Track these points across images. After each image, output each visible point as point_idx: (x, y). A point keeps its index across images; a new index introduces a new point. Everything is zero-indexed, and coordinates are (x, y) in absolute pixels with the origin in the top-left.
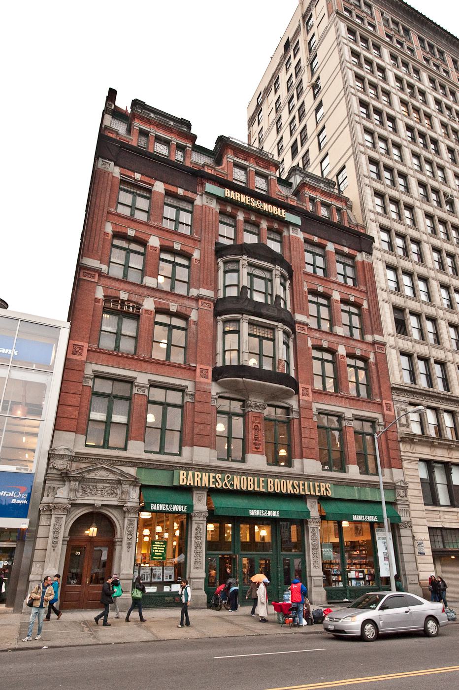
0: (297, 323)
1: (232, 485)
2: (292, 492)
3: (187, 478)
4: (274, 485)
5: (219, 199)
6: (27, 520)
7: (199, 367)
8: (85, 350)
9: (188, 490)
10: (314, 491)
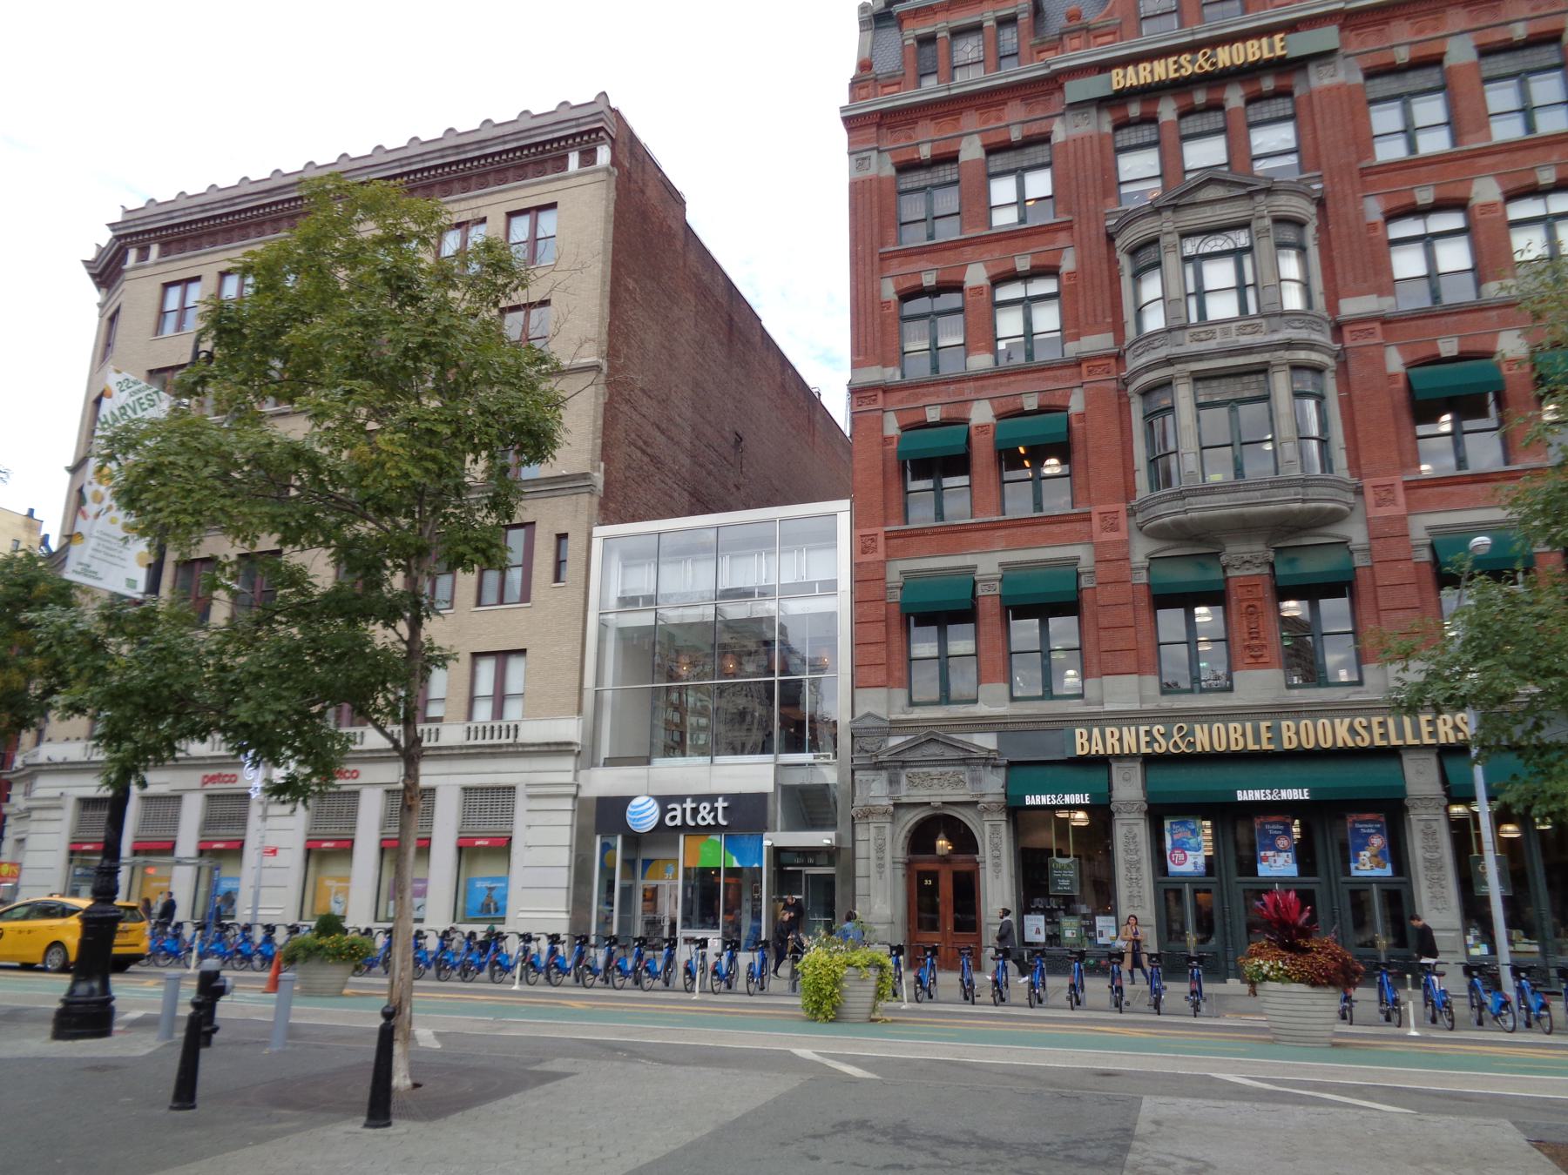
2: (1351, 744)
3: (1089, 740)
4: (1297, 733)
5: (1102, 103)
6: (832, 834)
7: (1095, 510)
8: (881, 539)
9: (1101, 762)
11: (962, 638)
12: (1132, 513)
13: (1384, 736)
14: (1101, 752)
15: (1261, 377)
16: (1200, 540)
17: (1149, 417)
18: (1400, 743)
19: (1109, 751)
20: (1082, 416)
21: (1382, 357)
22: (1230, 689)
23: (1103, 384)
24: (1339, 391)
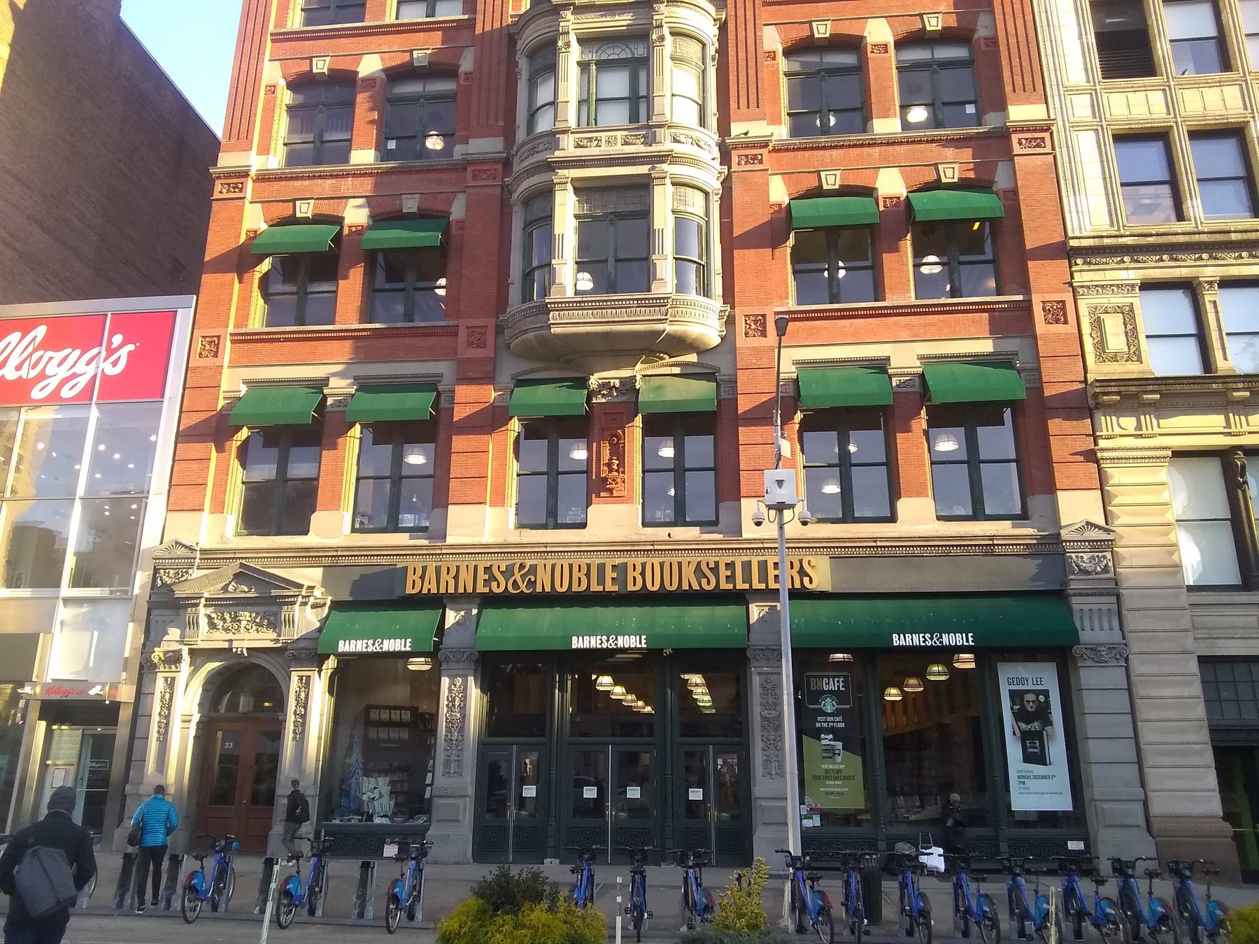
1: (532, 584)
2: (696, 587)
3: (422, 577)
4: (643, 574)
11: (308, 461)
12: (499, 330)
14: (434, 591)
16: (569, 362)
17: (528, 224)
18: (747, 586)
19: (442, 590)
20: (460, 223)
21: (767, 184)
22: (583, 526)
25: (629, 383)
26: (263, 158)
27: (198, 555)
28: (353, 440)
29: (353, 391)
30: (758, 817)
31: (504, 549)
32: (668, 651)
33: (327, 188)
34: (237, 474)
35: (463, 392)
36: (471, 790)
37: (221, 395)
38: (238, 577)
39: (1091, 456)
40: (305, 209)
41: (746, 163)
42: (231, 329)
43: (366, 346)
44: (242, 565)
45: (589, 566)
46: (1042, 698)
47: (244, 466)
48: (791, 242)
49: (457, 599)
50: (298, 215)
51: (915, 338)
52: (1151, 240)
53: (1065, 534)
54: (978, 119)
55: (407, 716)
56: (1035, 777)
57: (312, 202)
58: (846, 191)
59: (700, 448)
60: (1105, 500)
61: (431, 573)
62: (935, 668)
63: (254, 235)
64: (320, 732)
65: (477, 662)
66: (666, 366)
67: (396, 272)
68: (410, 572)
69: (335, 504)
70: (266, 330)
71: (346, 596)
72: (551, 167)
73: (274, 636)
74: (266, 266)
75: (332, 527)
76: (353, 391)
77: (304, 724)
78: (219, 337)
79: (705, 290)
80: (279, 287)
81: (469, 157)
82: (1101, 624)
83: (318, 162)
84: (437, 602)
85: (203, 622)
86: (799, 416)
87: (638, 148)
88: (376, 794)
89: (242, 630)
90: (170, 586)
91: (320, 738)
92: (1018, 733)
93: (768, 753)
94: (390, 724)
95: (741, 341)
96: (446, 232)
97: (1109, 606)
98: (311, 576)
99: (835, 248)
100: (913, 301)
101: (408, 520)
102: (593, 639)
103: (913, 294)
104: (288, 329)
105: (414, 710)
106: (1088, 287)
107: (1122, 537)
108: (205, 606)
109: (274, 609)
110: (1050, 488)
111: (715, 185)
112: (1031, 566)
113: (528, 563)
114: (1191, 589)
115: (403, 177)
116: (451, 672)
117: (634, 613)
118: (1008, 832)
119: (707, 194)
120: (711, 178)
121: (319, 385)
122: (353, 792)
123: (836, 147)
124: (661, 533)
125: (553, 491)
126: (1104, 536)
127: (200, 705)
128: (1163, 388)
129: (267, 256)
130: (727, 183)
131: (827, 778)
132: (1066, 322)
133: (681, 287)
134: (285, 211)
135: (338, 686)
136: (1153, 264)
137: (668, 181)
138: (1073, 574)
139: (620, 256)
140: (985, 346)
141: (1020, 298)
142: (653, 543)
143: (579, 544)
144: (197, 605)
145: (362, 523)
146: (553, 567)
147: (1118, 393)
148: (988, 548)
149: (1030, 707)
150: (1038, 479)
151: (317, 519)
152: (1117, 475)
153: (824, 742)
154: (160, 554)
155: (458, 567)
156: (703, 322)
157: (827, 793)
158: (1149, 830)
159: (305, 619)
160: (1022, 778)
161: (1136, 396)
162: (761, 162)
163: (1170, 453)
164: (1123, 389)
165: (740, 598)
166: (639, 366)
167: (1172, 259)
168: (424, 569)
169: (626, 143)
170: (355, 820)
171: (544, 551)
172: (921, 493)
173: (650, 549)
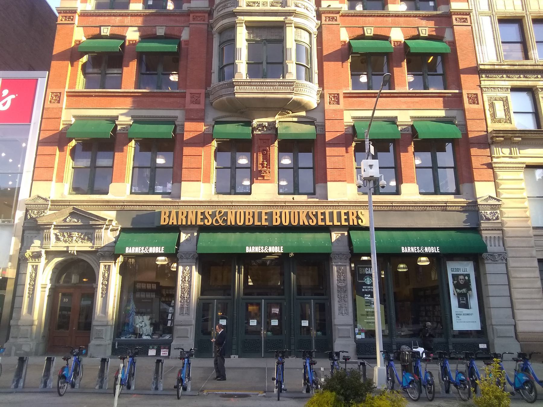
0: (324, 13)
1: (225, 221)
2: (306, 223)
3: (169, 217)
7: (188, 92)
10: (339, 220)
11: (107, 158)
12: (207, 95)
13: (324, 220)
14: (175, 223)
15: (280, 30)
16: (242, 113)
18: (331, 224)
19: (180, 223)
20: (187, 42)
21: (339, 31)
22: (250, 194)
23: (200, 26)
24: (317, 46)
25: (272, 126)
26: (84, 4)
27: (50, 203)
28: (131, 148)
29: (131, 123)
30: (336, 334)
31: (210, 204)
32: (292, 255)
33: (117, 21)
34: (70, 163)
35: (188, 126)
36: (194, 322)
37: (62, 123)
38: (72, 214)
39: (490, 166)
40: (106, 31)
41: (329, 20)
42: (67, 89)
43: (139, 101)
44: (74, 208)
45: (254, 213)
46: (467, 278)
47: (73, 159)
48: (350, 60)
49: (187, 228)
50: (102, 34)
51: (410, 109)
52: (516, 67)
53: (479, 202)
54: (435, 8)
55: (154, 287)
56: (464, 314)
57: (109, 28)
58: (376, 37)
59: (306, 159)
60: (497, 186)
61: (173, 214)
62: (402, 266)
63: (79, 43)
64: (115, 292)
65: (197, 259)
66: (290, 117)
67: (153, 65)
68: (163, 214)
69: (122, 179)
70: (85, 90)
71: (129, 225)
72: (234, 14)
73: (91, 245)
74: (85, 59)
75: (121, 190)
76: (131, 123)
77: (107, 289)
78: (60, 93)
79: (310, 79)
80: (90, 70)
81: (191, 9)
82: (495, 243)
83: (112, 8)
84: (176, 229)
85: (53, 237)
86: (354, 144)
87: (278, 8)
88: (143, 324)
89: (74, 241)
90: (35, 218)
91: (115, 296)
92: (456, 294)
93: (341, 303)
94: (146, 291)
95: (327, 106)
96: (179, 45)
97: (499, 235)
98: (111, 215)
99: (371, 63)
100: (407, 90)
101: (159, 188)
102: (257, 248)
103: (407, 87)
104: (97, 90)
105: (158, 284)
106: (488, 88)
107: (504, 203)
108: (54, 229)
109: (91, 231)
110: (472, 180)
111: (314, 30)
112: (463, 216)
113: (223, 211)
114: (535, 228)
115: (157, 18)
116: (183, 264)
117: (276, 236)
118: (452, 340)
119: (310, 34)
120: (312, 25)
121: (113, 119)
122: (130, 324)
123: (371, 16)
124: (289, 198)
125: (233, 177)
126: (497, 203)
127: (51, 279)
128: (523, 135)
129: (86, 53)
130: (320, 29)
131: (367, 315)
132: (478, 104)
133: (298, 77)
134: (96, 31)
135: (123, 270)
136: (516, 79)
137: (293, 25)
138: (483, 220)
139: (269, 61)
140: (442, 113)
141: (457, 91)
142: (285, 202)
143: (249, 202)
144: (50, 228)
145: (135, 190)
146: (236, 213)
147: (503, 137)
148: (444, 208)
149: (462, 282)
150: (464, 176)
151: (113, 187)
152: (501, 175)
153: (366, 298)
154: (29, 202)
155: (187, 212)
156: (309, 94)
157: (368, 323)
158: (516, 338)
159: (107, 237)
160: (458, 315)
161: (510, 139)
162: (336, 20)
163: (524, 166)
164: (505, 135)
165: (327, 229)
166: (277, 116)
167: (525, 77)
168: (170, 213)
169: (272, 6)
170: (133, 338)
171: (231, 205)
172: (412, 182)
173: (284, 205)
